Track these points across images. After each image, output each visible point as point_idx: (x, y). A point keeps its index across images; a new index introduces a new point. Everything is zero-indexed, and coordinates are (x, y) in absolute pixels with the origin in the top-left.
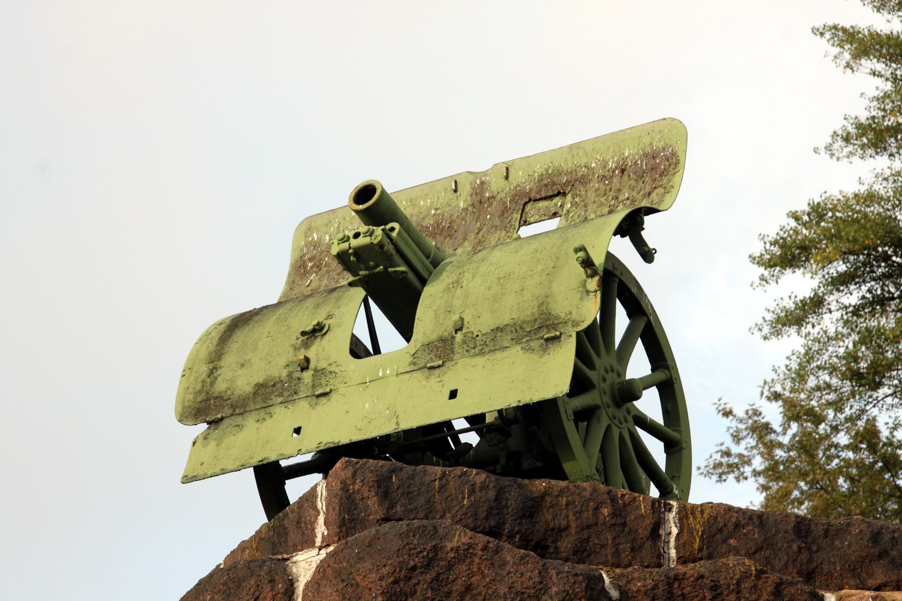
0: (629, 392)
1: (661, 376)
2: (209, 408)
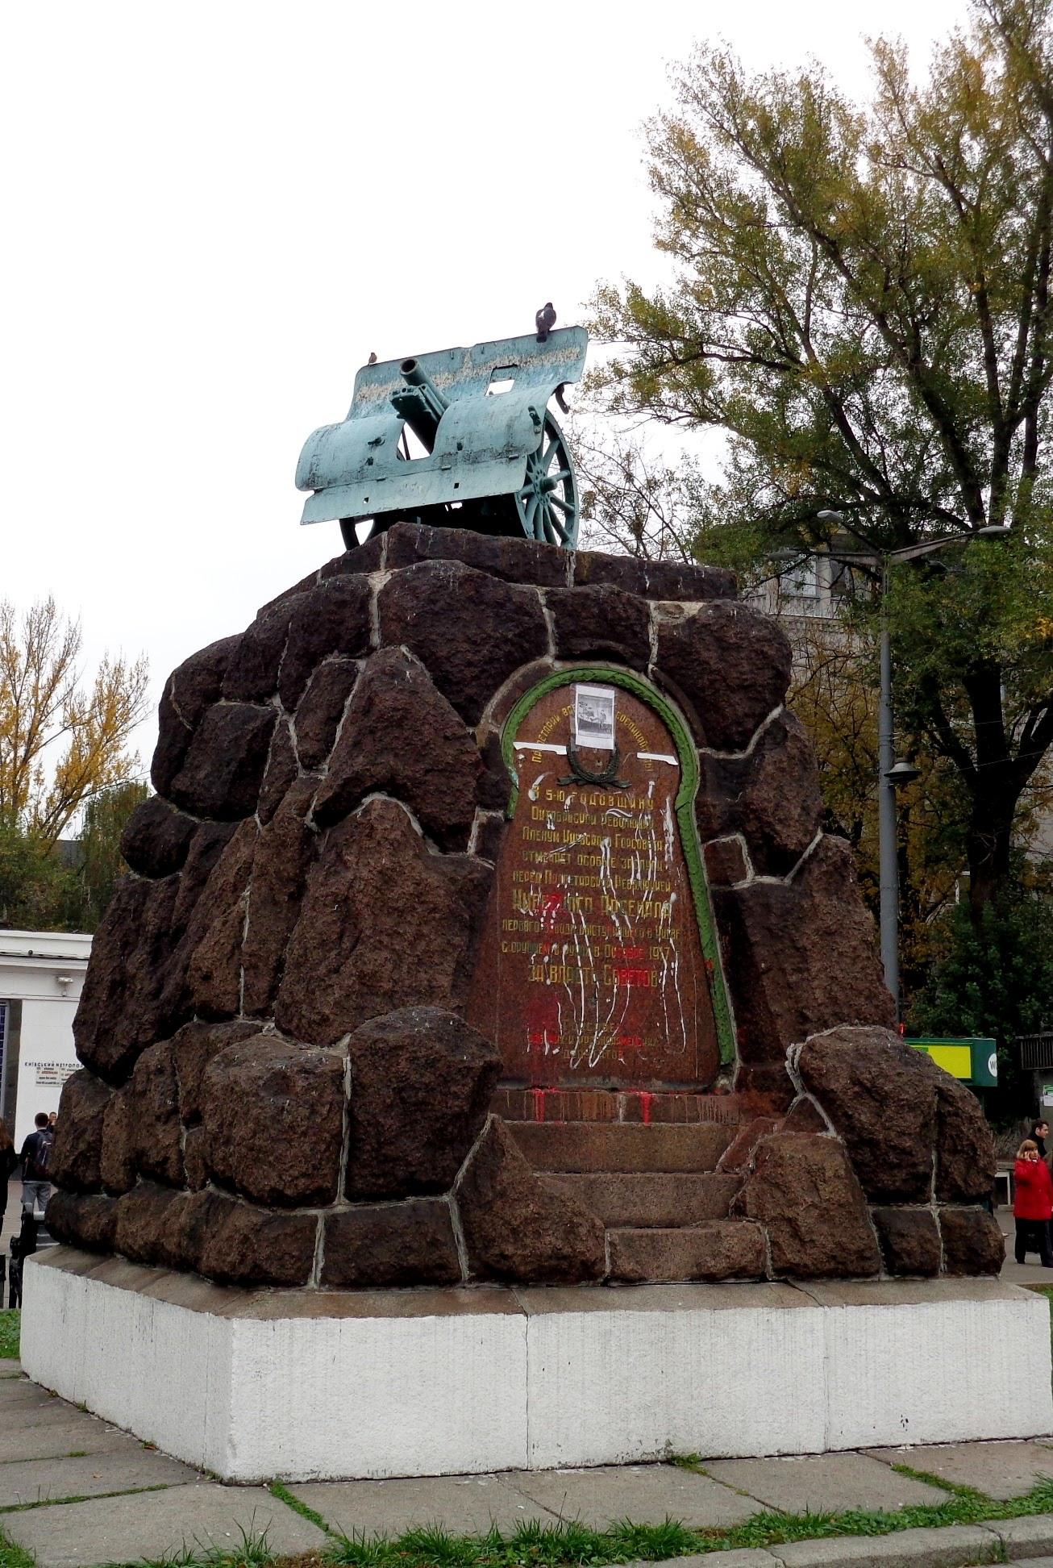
0: (548, 486)
1: (565, 473)
2: (313, 481)
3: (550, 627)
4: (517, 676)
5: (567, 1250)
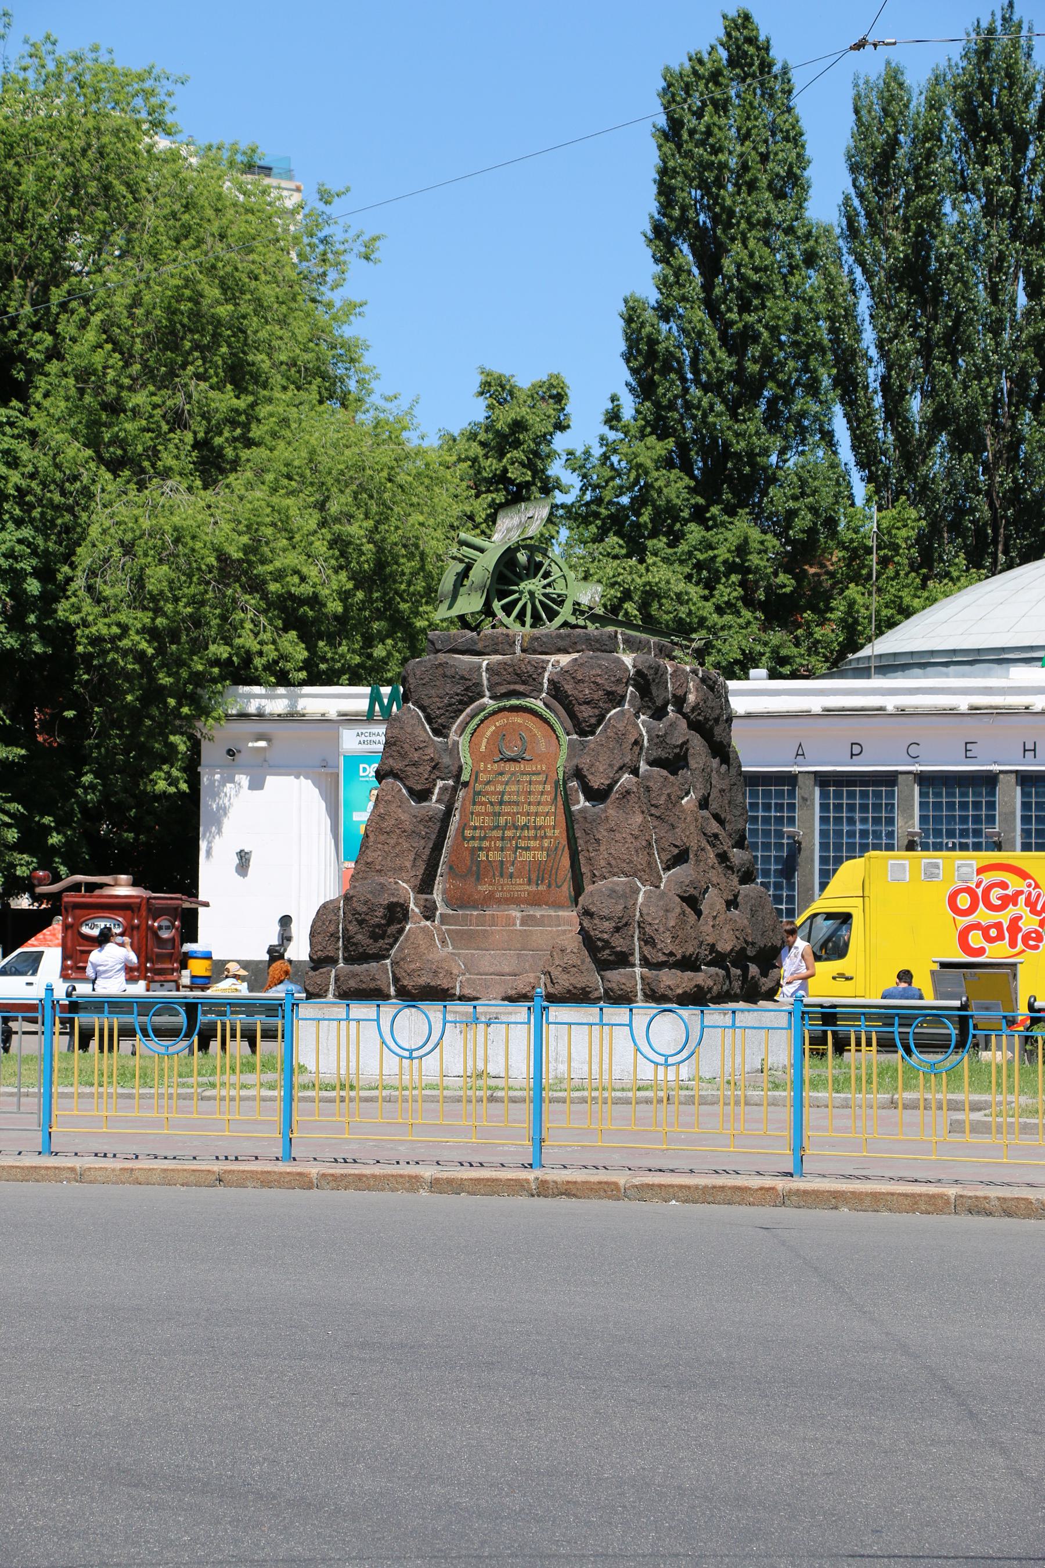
3: (485, 682)
4: (468, 710)
5: (433, 984)
